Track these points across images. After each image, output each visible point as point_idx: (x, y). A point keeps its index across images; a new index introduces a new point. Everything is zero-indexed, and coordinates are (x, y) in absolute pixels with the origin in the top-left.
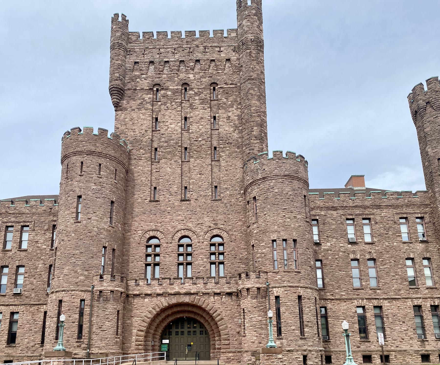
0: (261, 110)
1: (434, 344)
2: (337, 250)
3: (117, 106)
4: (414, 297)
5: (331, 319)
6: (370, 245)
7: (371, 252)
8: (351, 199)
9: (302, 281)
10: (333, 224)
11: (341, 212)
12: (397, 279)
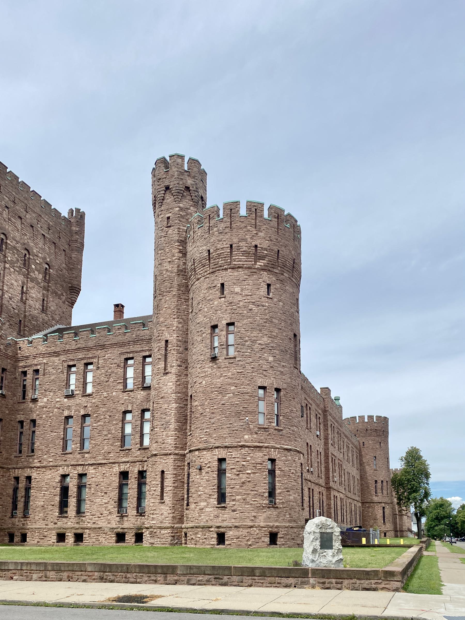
2: (52, 406)
5: (34, 491)
6: (88, 398)
7: (86, 406)
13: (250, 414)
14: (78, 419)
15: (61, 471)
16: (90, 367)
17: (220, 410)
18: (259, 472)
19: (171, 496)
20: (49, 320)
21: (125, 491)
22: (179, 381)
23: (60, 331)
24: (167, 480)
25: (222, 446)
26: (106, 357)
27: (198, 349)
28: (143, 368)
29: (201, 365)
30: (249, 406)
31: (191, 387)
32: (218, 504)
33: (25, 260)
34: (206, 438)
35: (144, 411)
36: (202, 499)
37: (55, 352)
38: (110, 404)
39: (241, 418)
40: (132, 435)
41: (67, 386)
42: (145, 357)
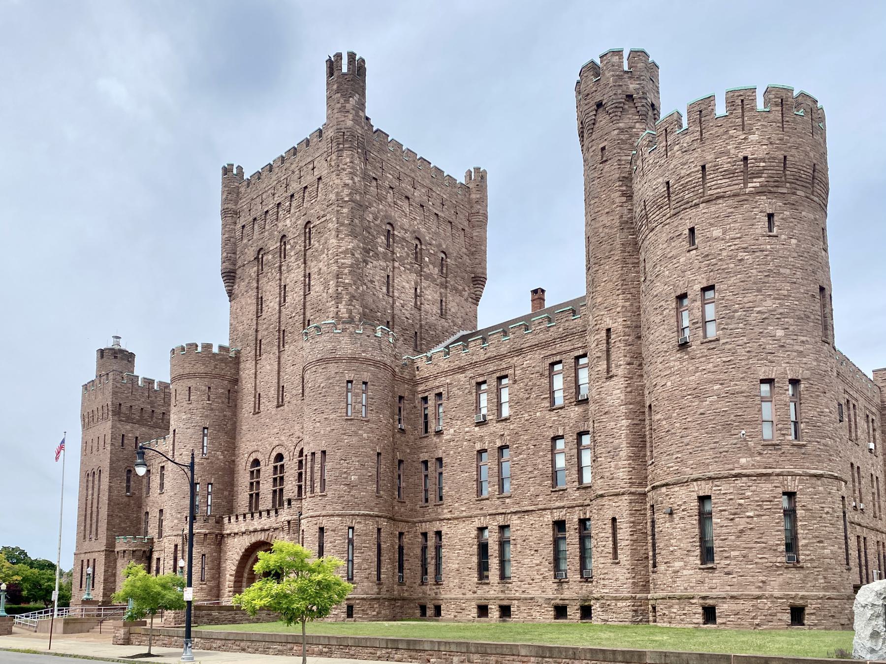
0: (340, 250)
1: (576, 587)
2: (461, 439)
3: (230, 293)
4: (554, 507)
7: (503, 435)
8: (483, 348)
9: (328, 507)
10: (460, 397)
11: (469, 373)
12: (535, 477)
13: (748, 424)
14: (494, 452)
15: (477, 523)
16: (505, 381)
17: (697, 422)
18: (768, 513)
19: (629, 553)
20: (450, 326)
21: (562, 547)
22: (630, 387)
23: (464, 338)
24: (621, 531)
25: (704, 477)
26: (524, 366)
27: (657, 335)
28: (575, 374)
29: (663, 358)
30: (746, 413)
31: (649, 393)
32: (702, 564)
33: (416, 253)
34: (677, 468)
35: (580, 435)
36: (676, 557)
37: (459, 368)
38: (533, 429)
39: (733, 432)
40: (567, 470)
41: (477, 410)
42: (577, 358)
